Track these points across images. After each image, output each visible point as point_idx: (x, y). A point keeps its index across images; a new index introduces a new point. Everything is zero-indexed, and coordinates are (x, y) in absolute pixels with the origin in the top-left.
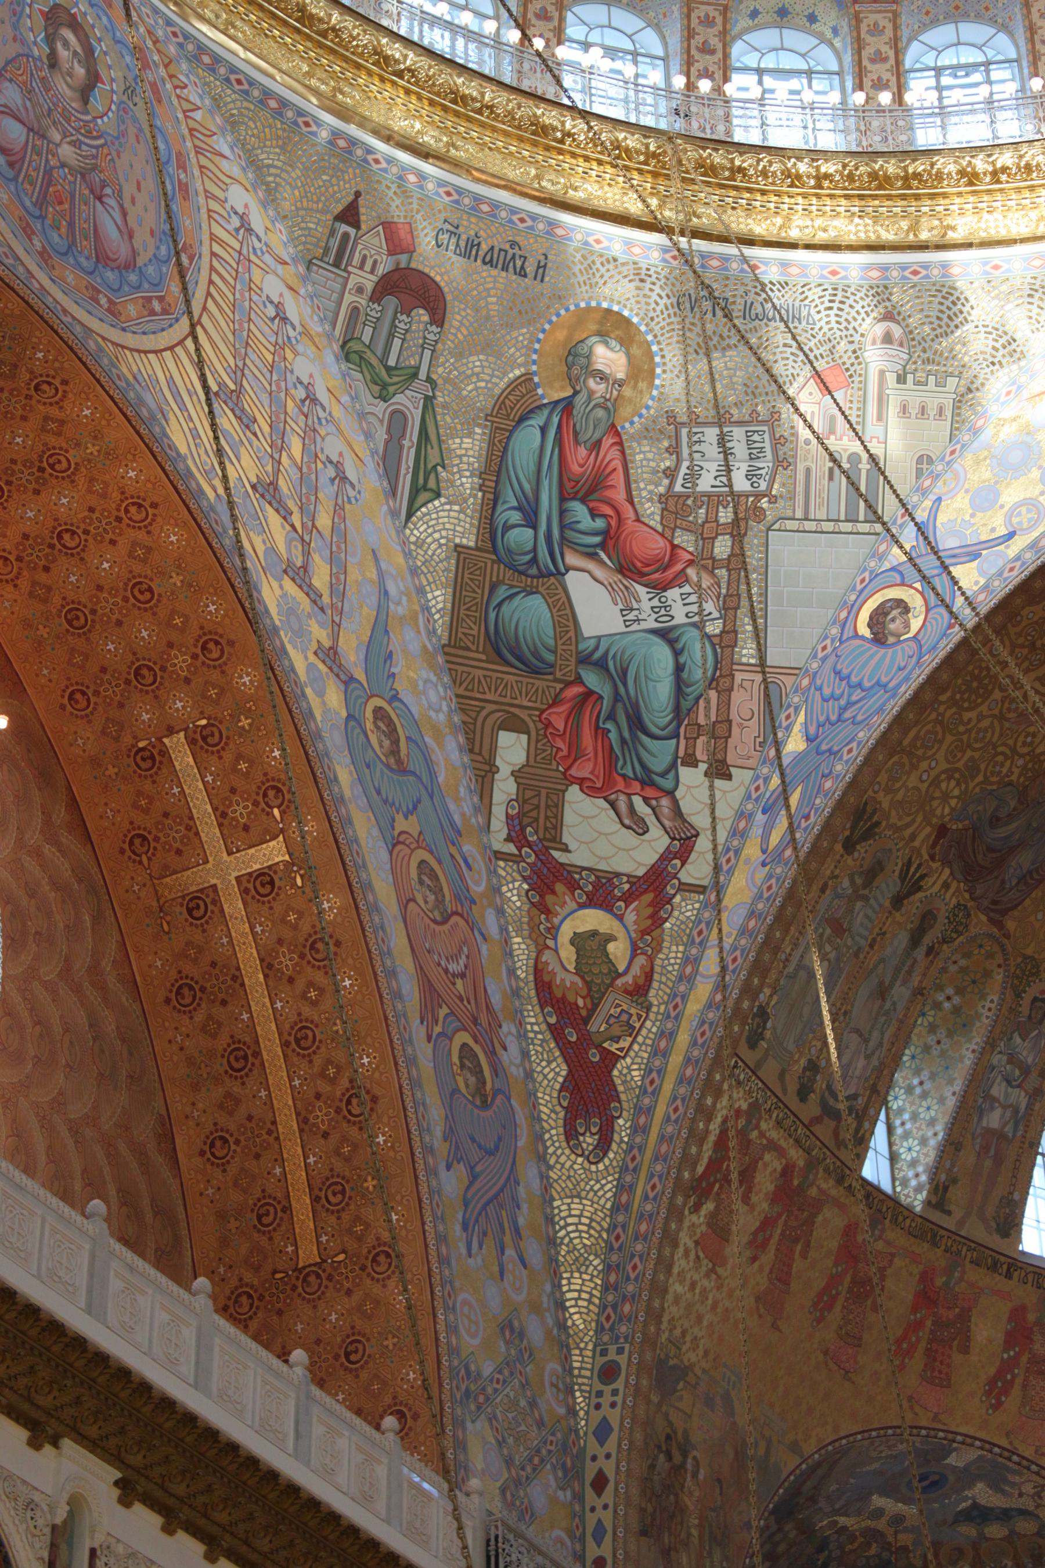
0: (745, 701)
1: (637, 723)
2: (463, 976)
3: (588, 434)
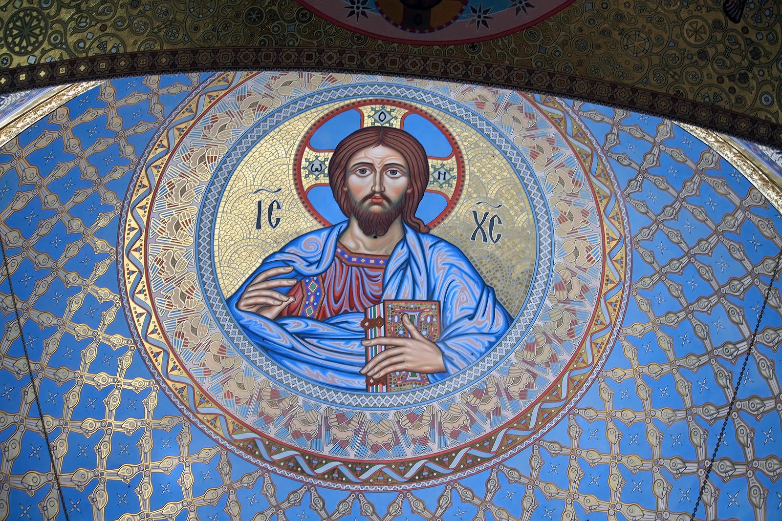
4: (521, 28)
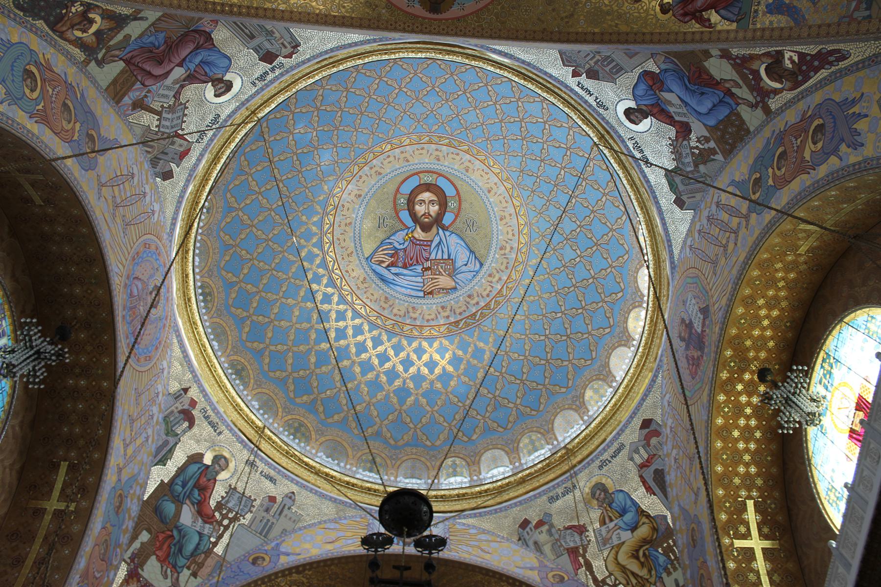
0: (210, 562)
1: (180, 551)
3: (209, 476)
4: (478, 10)
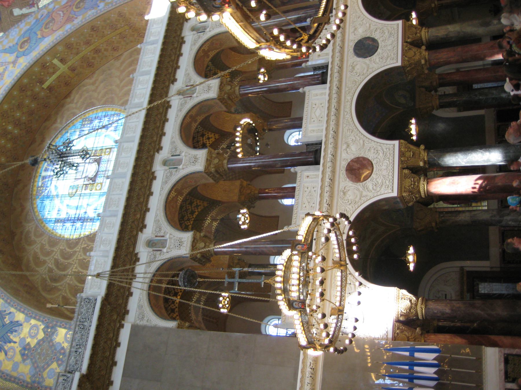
2: (63, 12)
